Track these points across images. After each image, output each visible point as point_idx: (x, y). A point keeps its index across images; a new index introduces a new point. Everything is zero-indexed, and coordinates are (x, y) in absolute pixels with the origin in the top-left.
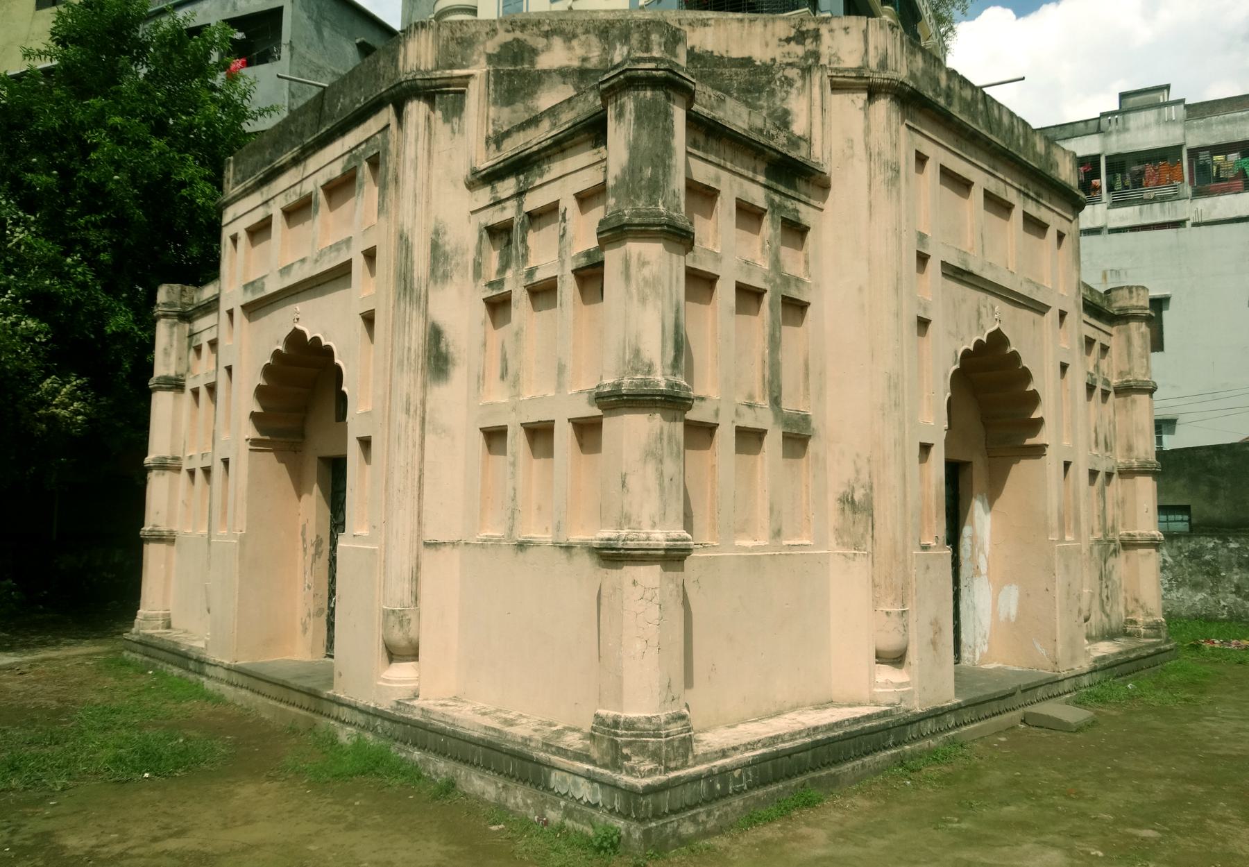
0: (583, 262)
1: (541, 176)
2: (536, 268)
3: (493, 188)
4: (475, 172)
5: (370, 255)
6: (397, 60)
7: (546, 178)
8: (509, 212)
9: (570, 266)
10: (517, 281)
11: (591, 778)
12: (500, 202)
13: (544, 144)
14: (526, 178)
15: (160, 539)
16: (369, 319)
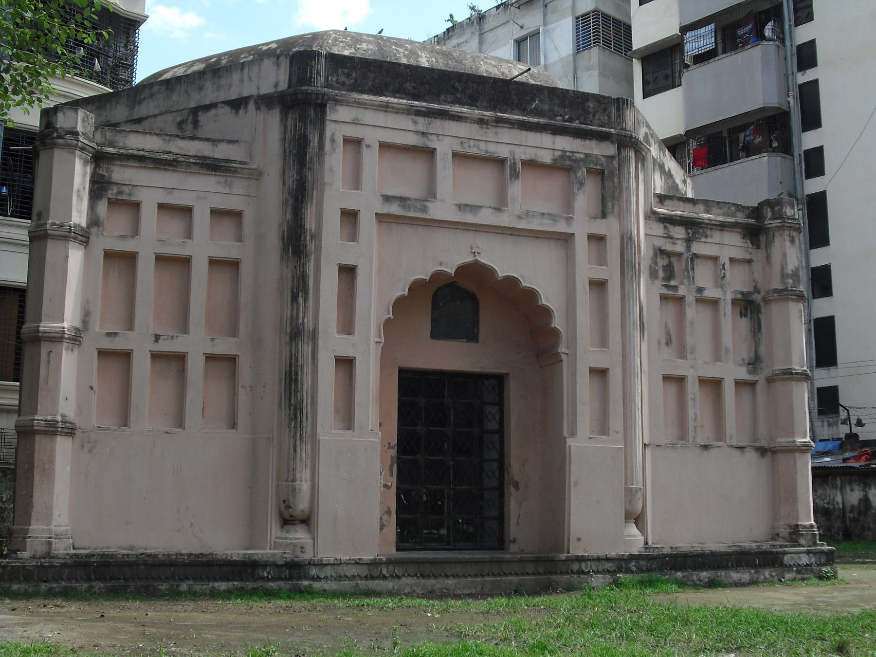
0: (739, 296)
1: (706, 237)
2: (704, 289)
3: (665, 227)
4: (655, 213)
5: (597, 239)
6: (611, 113)
7: (709, 240)
8: (680, 248)
9: (729, 297)
10: (690, 292)
11: (808, 553)
12: (671, 238)
13: (714, 222)
14: (694, 233)
15: (70, 431)
16: (598, 285)
